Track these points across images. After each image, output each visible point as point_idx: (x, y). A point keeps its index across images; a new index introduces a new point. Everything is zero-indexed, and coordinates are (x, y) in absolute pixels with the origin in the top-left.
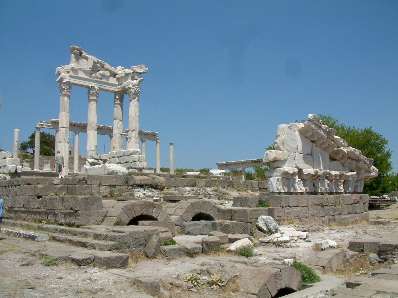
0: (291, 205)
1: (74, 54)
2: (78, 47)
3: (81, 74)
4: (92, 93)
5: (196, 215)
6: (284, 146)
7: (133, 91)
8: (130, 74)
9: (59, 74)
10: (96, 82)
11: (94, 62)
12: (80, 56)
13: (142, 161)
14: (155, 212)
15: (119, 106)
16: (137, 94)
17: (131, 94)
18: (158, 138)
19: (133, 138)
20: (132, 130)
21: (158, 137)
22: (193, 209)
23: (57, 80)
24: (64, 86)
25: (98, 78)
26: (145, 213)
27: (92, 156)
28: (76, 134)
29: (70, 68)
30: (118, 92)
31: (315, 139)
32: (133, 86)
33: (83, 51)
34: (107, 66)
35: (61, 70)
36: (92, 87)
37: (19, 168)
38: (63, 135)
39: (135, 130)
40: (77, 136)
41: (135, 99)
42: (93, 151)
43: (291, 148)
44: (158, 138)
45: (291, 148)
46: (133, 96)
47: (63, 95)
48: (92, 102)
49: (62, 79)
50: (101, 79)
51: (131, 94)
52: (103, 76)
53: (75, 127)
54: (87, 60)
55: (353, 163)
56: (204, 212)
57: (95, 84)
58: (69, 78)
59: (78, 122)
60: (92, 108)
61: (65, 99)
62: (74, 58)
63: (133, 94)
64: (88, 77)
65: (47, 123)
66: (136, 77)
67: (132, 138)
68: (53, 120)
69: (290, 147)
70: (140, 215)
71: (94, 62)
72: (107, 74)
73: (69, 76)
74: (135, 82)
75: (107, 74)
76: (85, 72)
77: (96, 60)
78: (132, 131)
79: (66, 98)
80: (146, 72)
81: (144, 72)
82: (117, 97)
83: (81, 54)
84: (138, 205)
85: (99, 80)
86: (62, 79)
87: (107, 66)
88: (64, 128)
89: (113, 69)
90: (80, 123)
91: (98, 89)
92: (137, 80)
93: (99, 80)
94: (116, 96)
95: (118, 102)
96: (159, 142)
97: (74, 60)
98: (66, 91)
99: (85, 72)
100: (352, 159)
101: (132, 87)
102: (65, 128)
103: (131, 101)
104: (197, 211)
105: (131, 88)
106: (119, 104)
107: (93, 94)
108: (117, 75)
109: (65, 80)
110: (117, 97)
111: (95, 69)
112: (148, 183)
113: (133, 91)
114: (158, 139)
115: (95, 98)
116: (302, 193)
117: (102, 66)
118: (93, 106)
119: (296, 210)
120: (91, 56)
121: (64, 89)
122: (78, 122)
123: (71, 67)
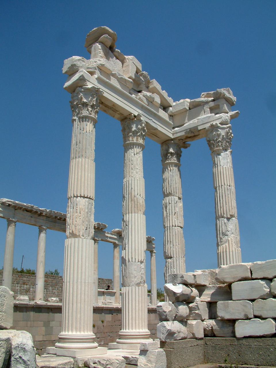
1: (101, 43)
2: (110, 30)
4: (134, 128)
7: (223, 133)
8: (207, 103)
9: (73, 70)
12: (110, 52)
15: (175, 169)
16: (228, 139)
17: (220, 139)
18: (153, 246)
19: (232, 233)
20: (229, 216)
21: (154, 245)
23: (67, 84)
24: (86, 98)
27: (182, 277)
28: (40, 231)
29: (95, 65)
30: (172, 140)
32: (221, 124)
35: (79, 63)
36: (135, 116)
37: (24, 350)
38: (81, 217)
39: (232, 216)
40: (43, 235)
41: (226, 150)
42: (142, 262)
44: (153, 246)
46: (224, 144)
47: (83, 119)
48: (137, 150)
49: (82, 79)
51: (220, 139)
52: (151, 101)
53: (41, 218)
54: (123, 64)
58: (96, 83)
59: (48, 210)
60: (135, 163)
61: (88, 127)
62: (101, 51)
63: (223, 138)
66: (226, 107)
67: (228, 233)
68: (5, 200)
72: (158, 100)
73: (96, 79)
74: (225, 116)
75: (158, 100)
76: (121, 81)
78: (228, 219)
79: (89, 127)
82: (171, 150)
83: (111, 48)
86: (82, 79)
88: (84, 197)
90: (51, 211)
92: (227, 113)
94: (169, 148)
95: (174, 160)
96: (155, 253)
97: (101, 55)
98: (90, 109)
99: (121, 81)
101: (219, 125)
102: (86, 199)
103: (219, 154)
105: (218, 127)
106: (176, 165)
107: (137, 133)
108: (171, 108)
109: (88, 83)
110: (171, 150)
113: (223, 133)
114: (154, 248)
115: (141, 141)
120: (132, 56)
121: (85, 105)
122: (48, 210)
123: (99, 62)
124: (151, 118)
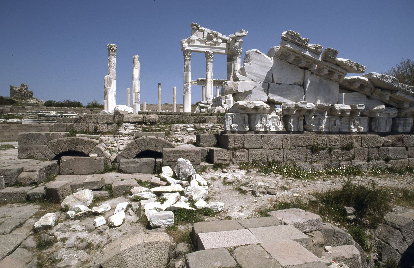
0: (247, 145)
3: (197, 43)
5: (141, 152)
6: (245, 75)
10: (210, 47)
11: (208, 33)
13: (228, 103)
14: (86, 149)
22: (137, 146)
25: (212, 45)
26: (73, 149)
31: (303, 64)
33: (199, 26)
34: (219, 35)
36: (207, 52)
43: (259, 77)
45: (259, 77)
50: (215, 45)
55: (385, 94)
56: (153, 150)
57: (210, 49)
58: (188, 47)
64: (204, 45)
65: (194, 81)
69: (256, 76)
70: (67, 150)
71: (208, 33)
75: (220, 40)
77: (209, 31)
80: (246, 35)
81: (244, 36)
84: (64, 142)
85: (213, 46)
87: (219, 35)
89: (224, 37)
91: (213, 53)
93: (213, 46)
100: (382, 89)
104: (144, 149)
111: (210, 38)
112: (138, 121)
116: (278, 132)
117: (216, 36)
118: (211, 65)
119: (256, 152)
124: (215, 49)
